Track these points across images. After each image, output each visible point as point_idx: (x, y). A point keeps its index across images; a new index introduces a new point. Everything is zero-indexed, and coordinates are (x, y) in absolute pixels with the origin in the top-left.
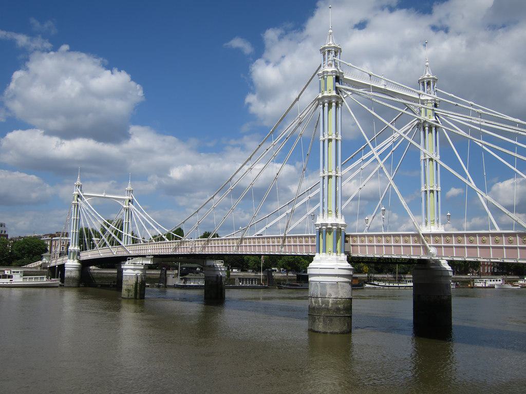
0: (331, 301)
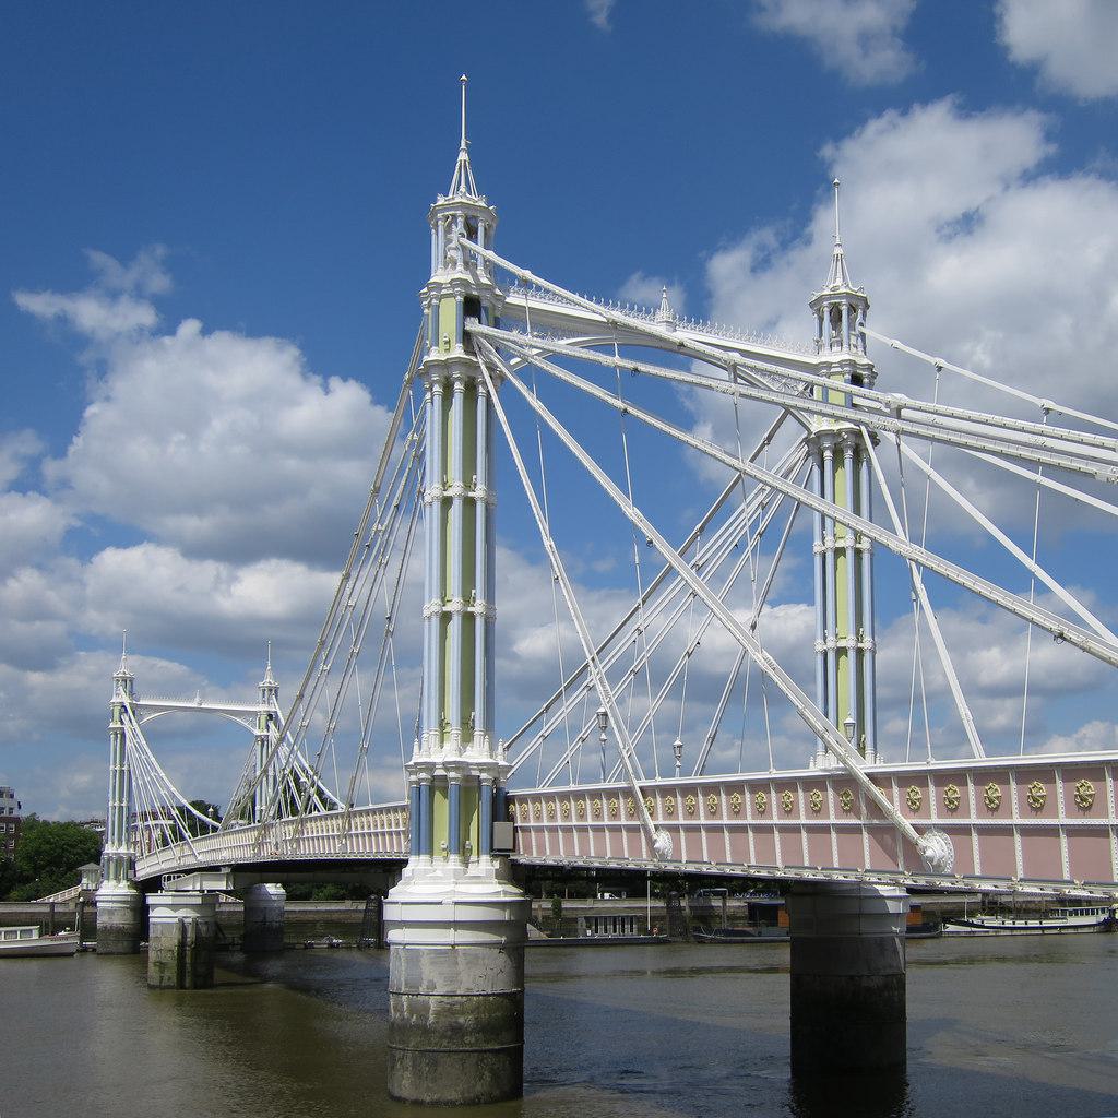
0: (433, 1002)
